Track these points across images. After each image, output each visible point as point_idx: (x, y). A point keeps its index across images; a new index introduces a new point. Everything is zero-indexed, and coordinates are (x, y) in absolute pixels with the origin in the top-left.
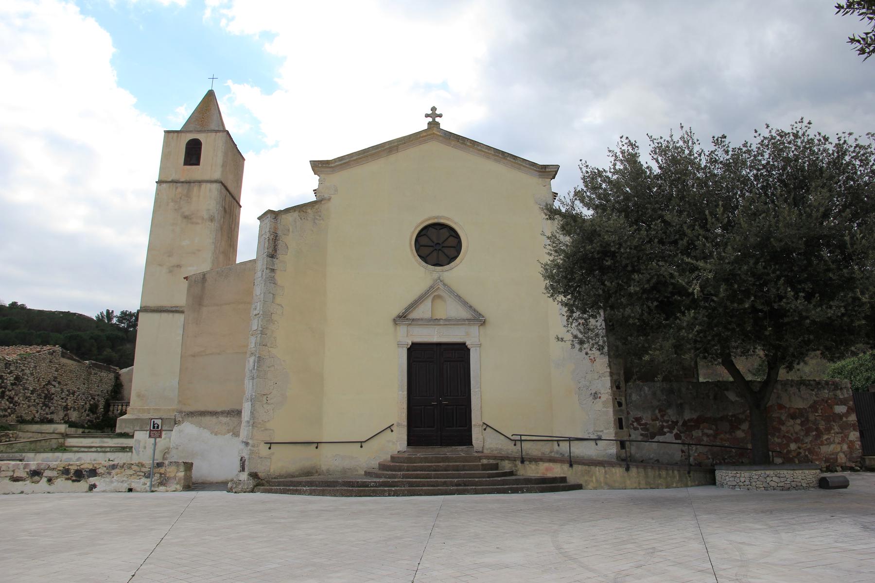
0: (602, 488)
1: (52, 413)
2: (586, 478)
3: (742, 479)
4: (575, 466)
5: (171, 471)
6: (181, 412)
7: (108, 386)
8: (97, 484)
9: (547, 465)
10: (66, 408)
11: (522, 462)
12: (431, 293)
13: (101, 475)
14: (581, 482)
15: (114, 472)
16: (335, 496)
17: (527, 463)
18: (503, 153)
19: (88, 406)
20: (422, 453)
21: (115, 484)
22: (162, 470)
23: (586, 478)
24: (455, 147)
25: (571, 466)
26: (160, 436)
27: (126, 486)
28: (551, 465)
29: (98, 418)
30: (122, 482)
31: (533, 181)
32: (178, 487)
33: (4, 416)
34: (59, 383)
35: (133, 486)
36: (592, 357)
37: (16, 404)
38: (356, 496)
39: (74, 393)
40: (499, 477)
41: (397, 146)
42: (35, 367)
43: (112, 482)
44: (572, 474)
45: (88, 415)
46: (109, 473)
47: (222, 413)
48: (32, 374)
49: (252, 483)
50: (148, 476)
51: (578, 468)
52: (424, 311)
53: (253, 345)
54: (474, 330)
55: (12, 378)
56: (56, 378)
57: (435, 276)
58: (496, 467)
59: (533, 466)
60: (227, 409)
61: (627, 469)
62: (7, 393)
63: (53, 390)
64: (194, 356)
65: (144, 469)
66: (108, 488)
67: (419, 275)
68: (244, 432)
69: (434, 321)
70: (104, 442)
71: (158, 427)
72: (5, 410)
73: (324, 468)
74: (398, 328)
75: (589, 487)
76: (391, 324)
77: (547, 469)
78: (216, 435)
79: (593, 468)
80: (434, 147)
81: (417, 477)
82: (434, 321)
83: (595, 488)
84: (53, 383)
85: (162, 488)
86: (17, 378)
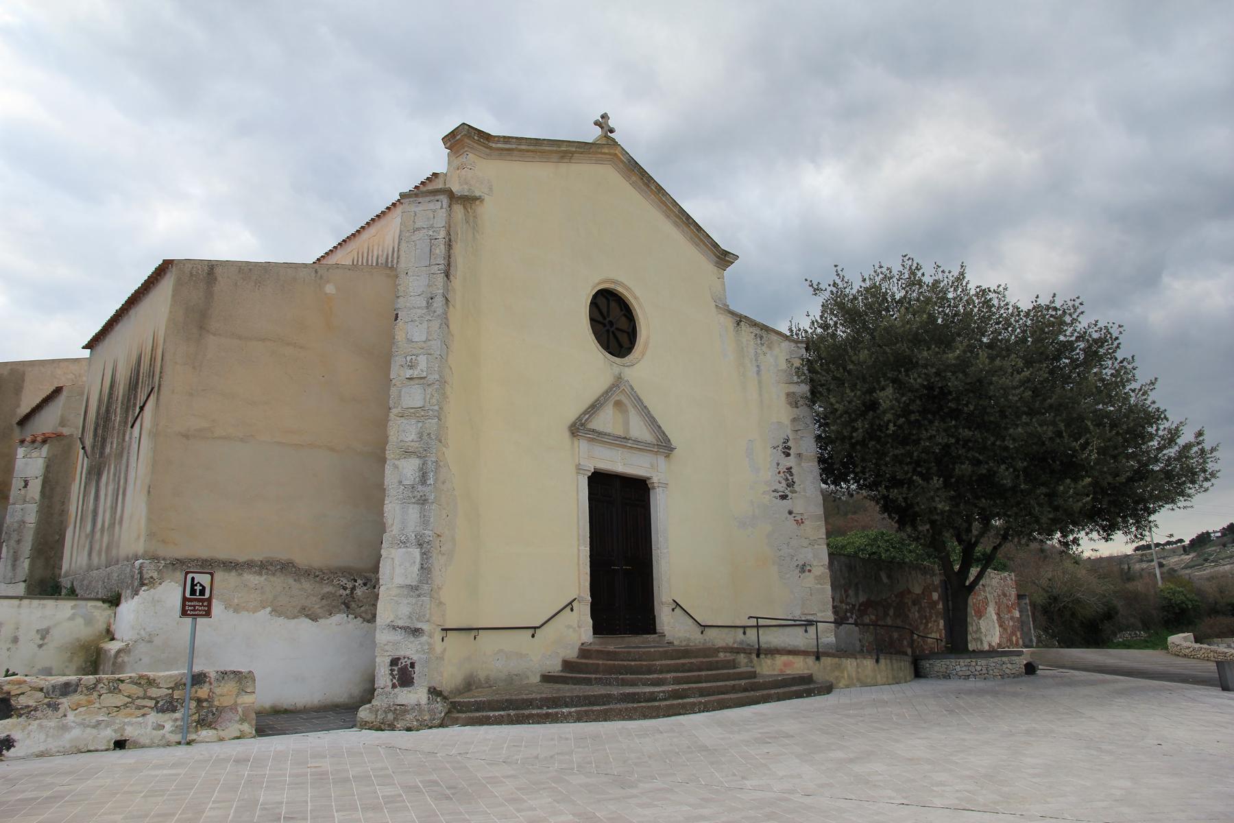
0: (855, 686)
2: (837, 673)
3: (979, 668)
4: (823, 659)
5: (225, 693)
6: (155, 558)
8: (16, 735)
9: (785, 658)
11: (758, 656)
12: (616, 395)
13: (28, 712)
14: (831, 678)
15: (65, 702)
16: (631, 718)
17: (762, 656)
18: (688, 217)
20: (614, 644)
21: (76, 732)
22: (203, 692)
23: (837, 673)
24: (633, 184)
25: (818, 658)
26: (208, 614)
27: (110, 734)
28: (791, 658)
30: (97, 725)
31: (705, 264)
32: (246, 727)
35: (130, 732)
36: (798, 518)
38: (664, 716)
40: (723, 677)
41: (573, 153)
43: (65, 728)
44: (818, 670)
46: (54, 707)
47: (249, 565)
49: (440, 707)
50: (169, 706)
51: (827, 661)
52: (606, 421)
53: (413, 436)
54: (661, 460)
57: (616, 370)
58: (733, 664)
59: (769, 662)
60: (258, 557)
61: (877, 661)
64: (187, 437)
65: (153, 692)
66: (53, 745)
67: (592, 366)
68: (391, 607)
69: (622, 442)
71: (202, 592)
73: (482, 675)
74: (576, 442)
75: (841, 685)
76: (567, 434)
77: (785, 665)
78: (236, 611)
79: (844, 660)
80: (609, 174)
81: (708, 679)
82: (622, 442)
83: (847, 686)
85: (205, 733)
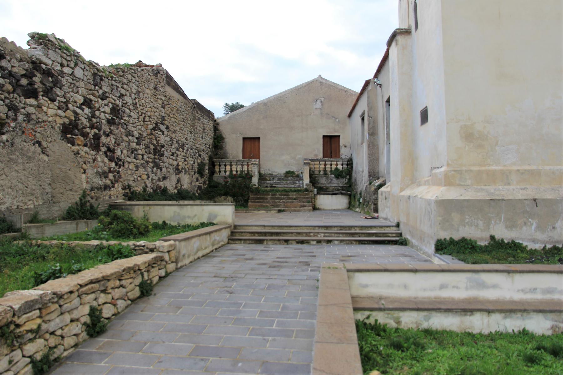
1: (164, 178)
7: (209, 140)
10: (178, 170)
19: (196, 166)
29: (204, 183)
33: (106, 187)
34: (167, 128)
37: (119, 162)
39: (183, 146)
42: (138, 92)
45: (197, 180)
48: (134, 105)
55: (107, 109)
56: (163, 118)
62: (104, 139)
63: (163, 139)
70: (483, 286)
72: (105, 175)
84: (163, 127)
86: (115, 110)
